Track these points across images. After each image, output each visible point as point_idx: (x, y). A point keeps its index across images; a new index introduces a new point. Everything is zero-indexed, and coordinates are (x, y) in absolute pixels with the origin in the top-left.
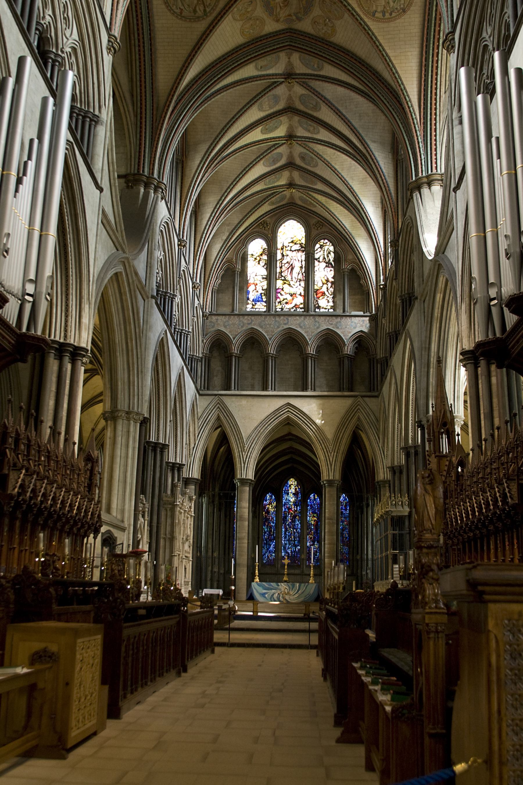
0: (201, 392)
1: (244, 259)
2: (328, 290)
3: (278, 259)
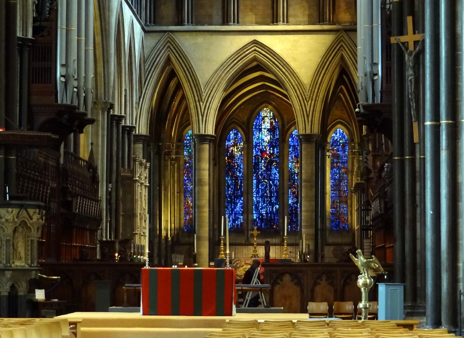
0: (146, 28)
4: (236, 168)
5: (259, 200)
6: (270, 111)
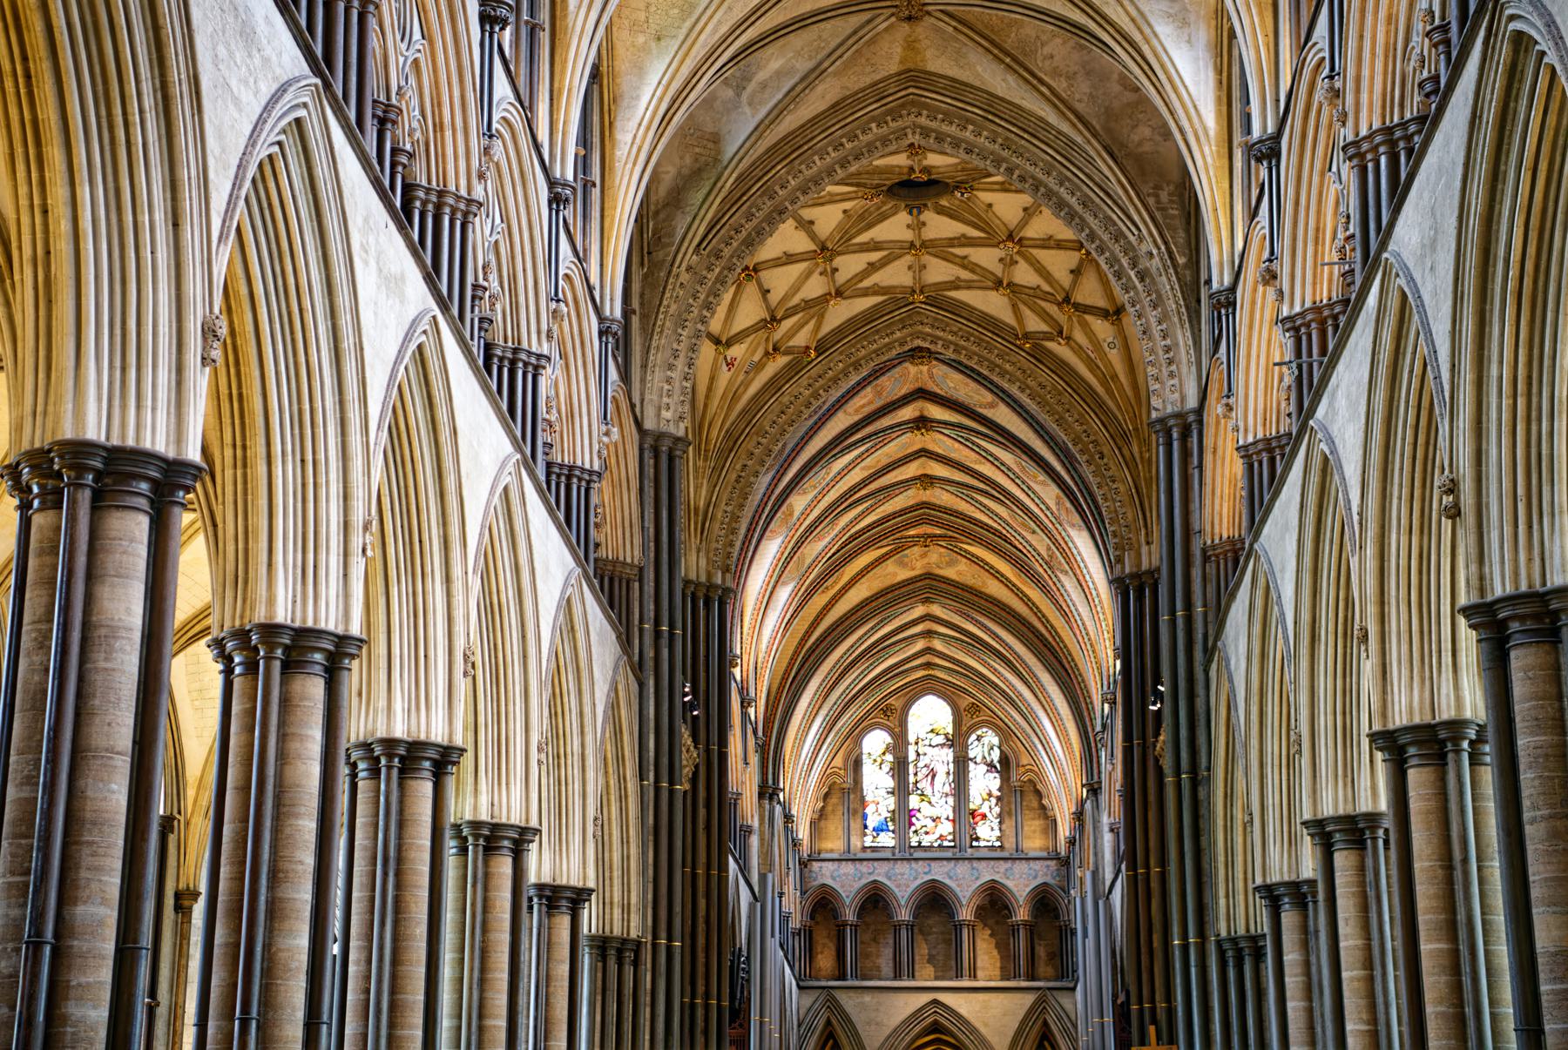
1: (857, 764)
2: (991, 809)
3: (910, 759)
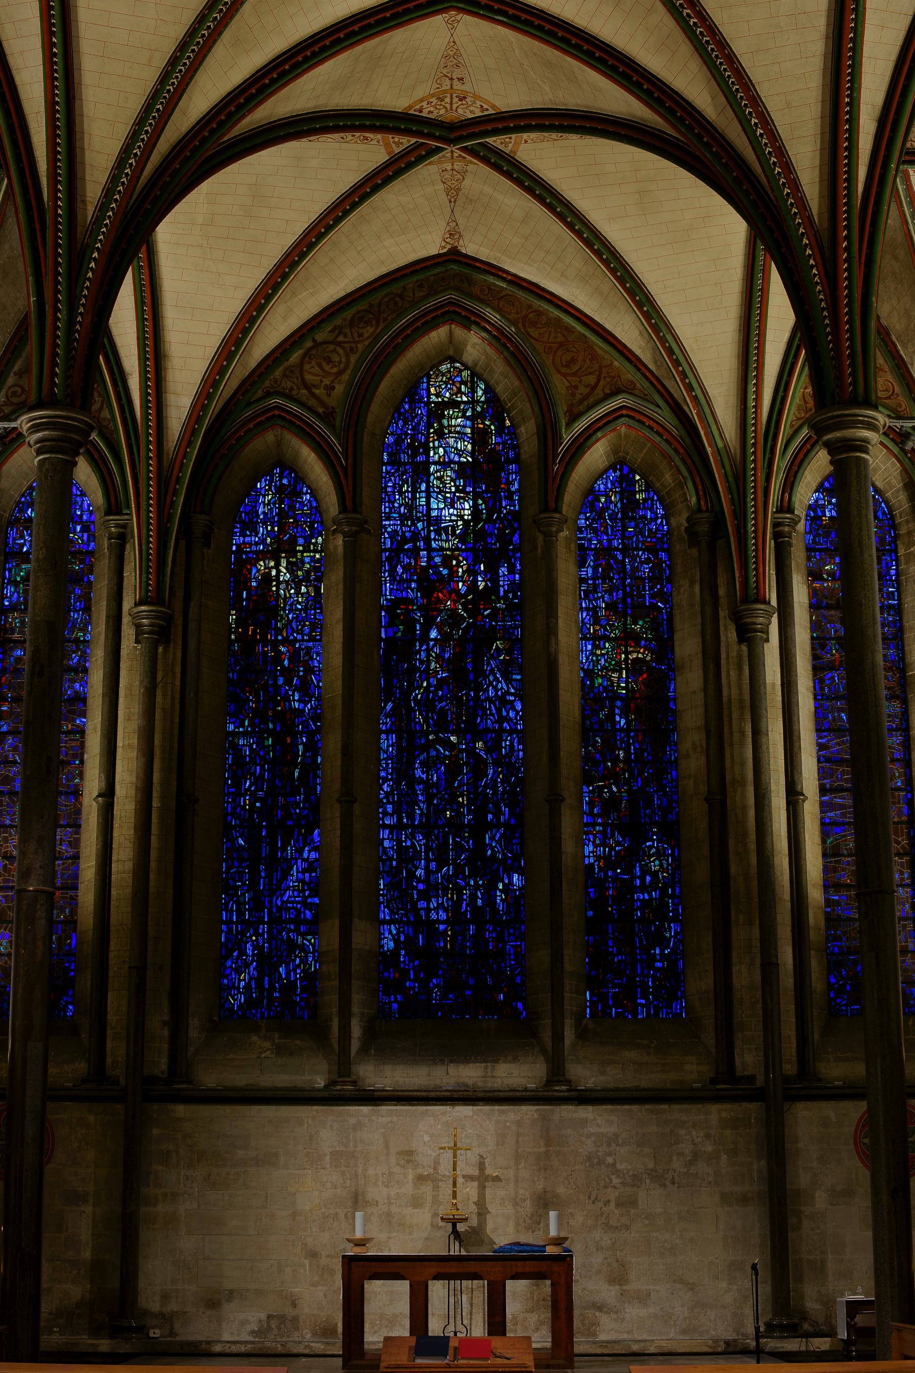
4: (288, 674)
5: (413, 844)
6: (473, 375)
